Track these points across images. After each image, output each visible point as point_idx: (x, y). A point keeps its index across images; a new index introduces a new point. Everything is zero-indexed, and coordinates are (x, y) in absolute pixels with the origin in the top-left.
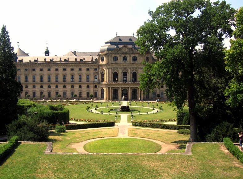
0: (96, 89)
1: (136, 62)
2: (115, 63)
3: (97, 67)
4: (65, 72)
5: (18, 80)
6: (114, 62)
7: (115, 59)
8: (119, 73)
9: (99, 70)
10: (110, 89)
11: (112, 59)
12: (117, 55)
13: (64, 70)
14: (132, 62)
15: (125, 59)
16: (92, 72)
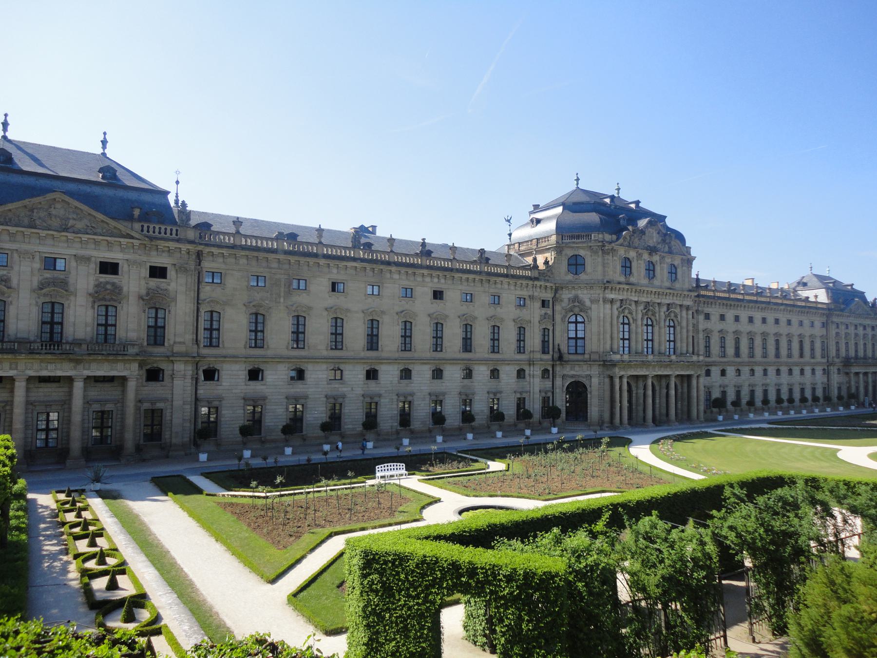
0: (548, 384)
1: (677, 285)
2: (627, 284)
3: (548, 296)
4: (437, 307)
5: (207, 334)
6: (622, 279)
7: (627, 265)
8: (635, 320)
9: (558, 308)
10: (625, 380)
11: (619, 268)
12: (632, 254)
13: (438, 295)
14: (667, 284)
15: (651, 270)
16: (535, 312)
